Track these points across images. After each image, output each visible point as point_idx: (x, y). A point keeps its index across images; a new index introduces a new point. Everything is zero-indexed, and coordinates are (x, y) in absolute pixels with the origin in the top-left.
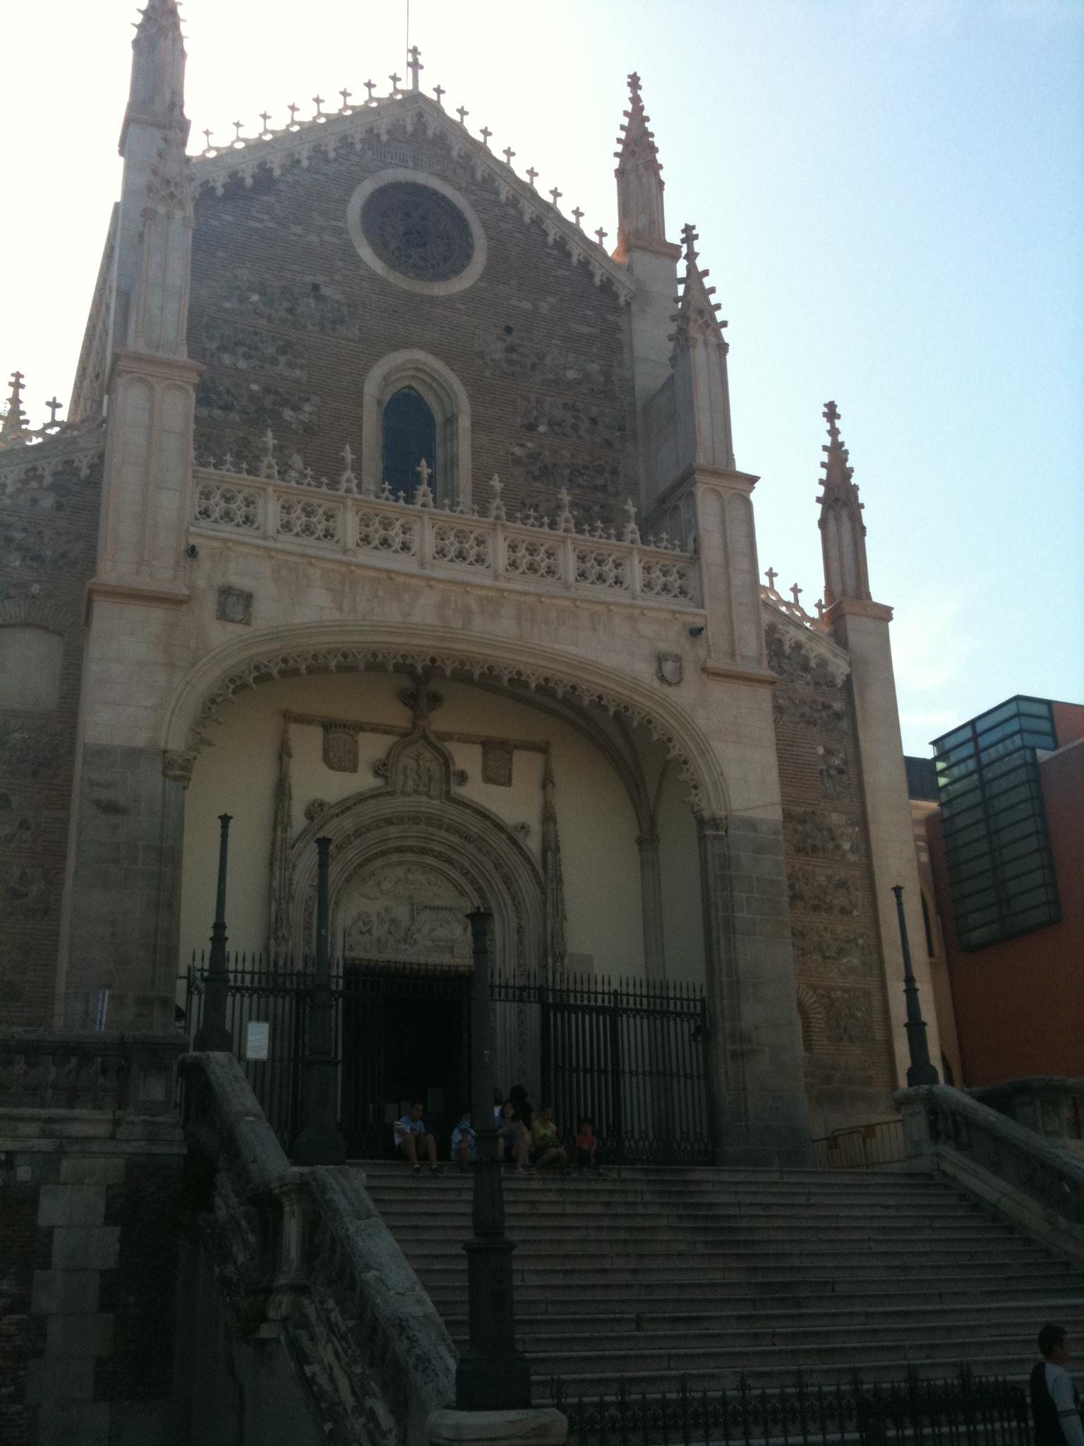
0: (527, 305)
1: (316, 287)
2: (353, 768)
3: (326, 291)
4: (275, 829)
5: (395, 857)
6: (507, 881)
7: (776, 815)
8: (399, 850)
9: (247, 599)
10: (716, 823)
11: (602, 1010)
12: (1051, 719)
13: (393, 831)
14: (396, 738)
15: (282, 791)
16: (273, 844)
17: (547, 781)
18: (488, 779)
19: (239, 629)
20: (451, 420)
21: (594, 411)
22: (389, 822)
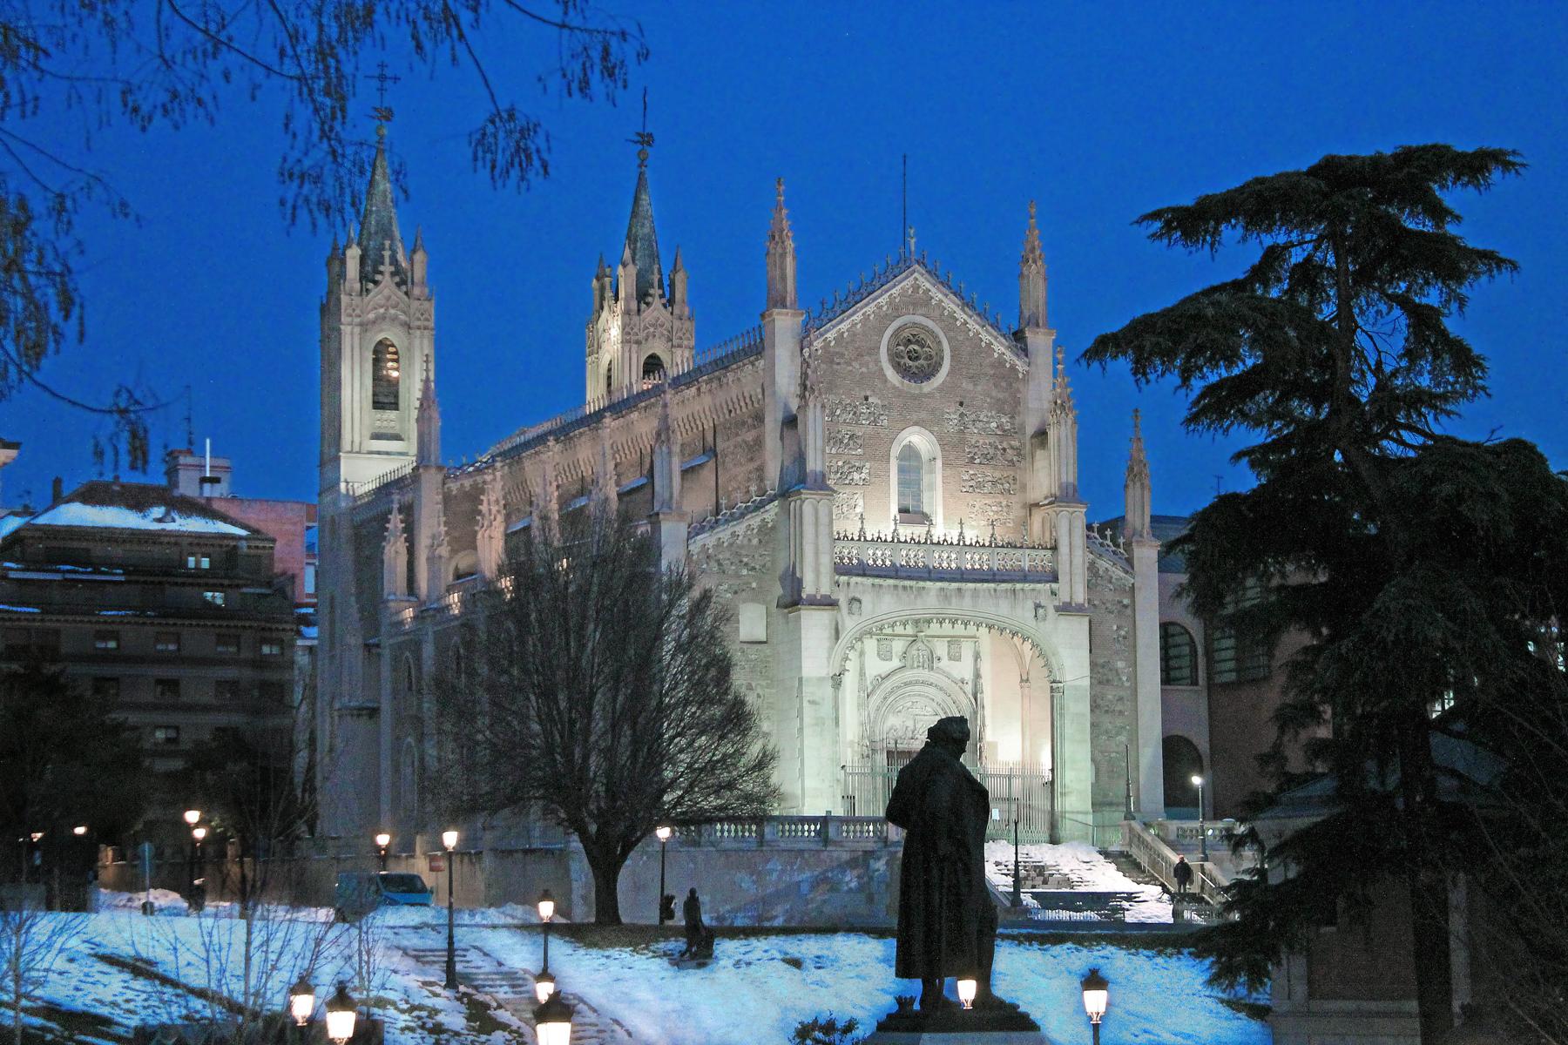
17: (977, 657)
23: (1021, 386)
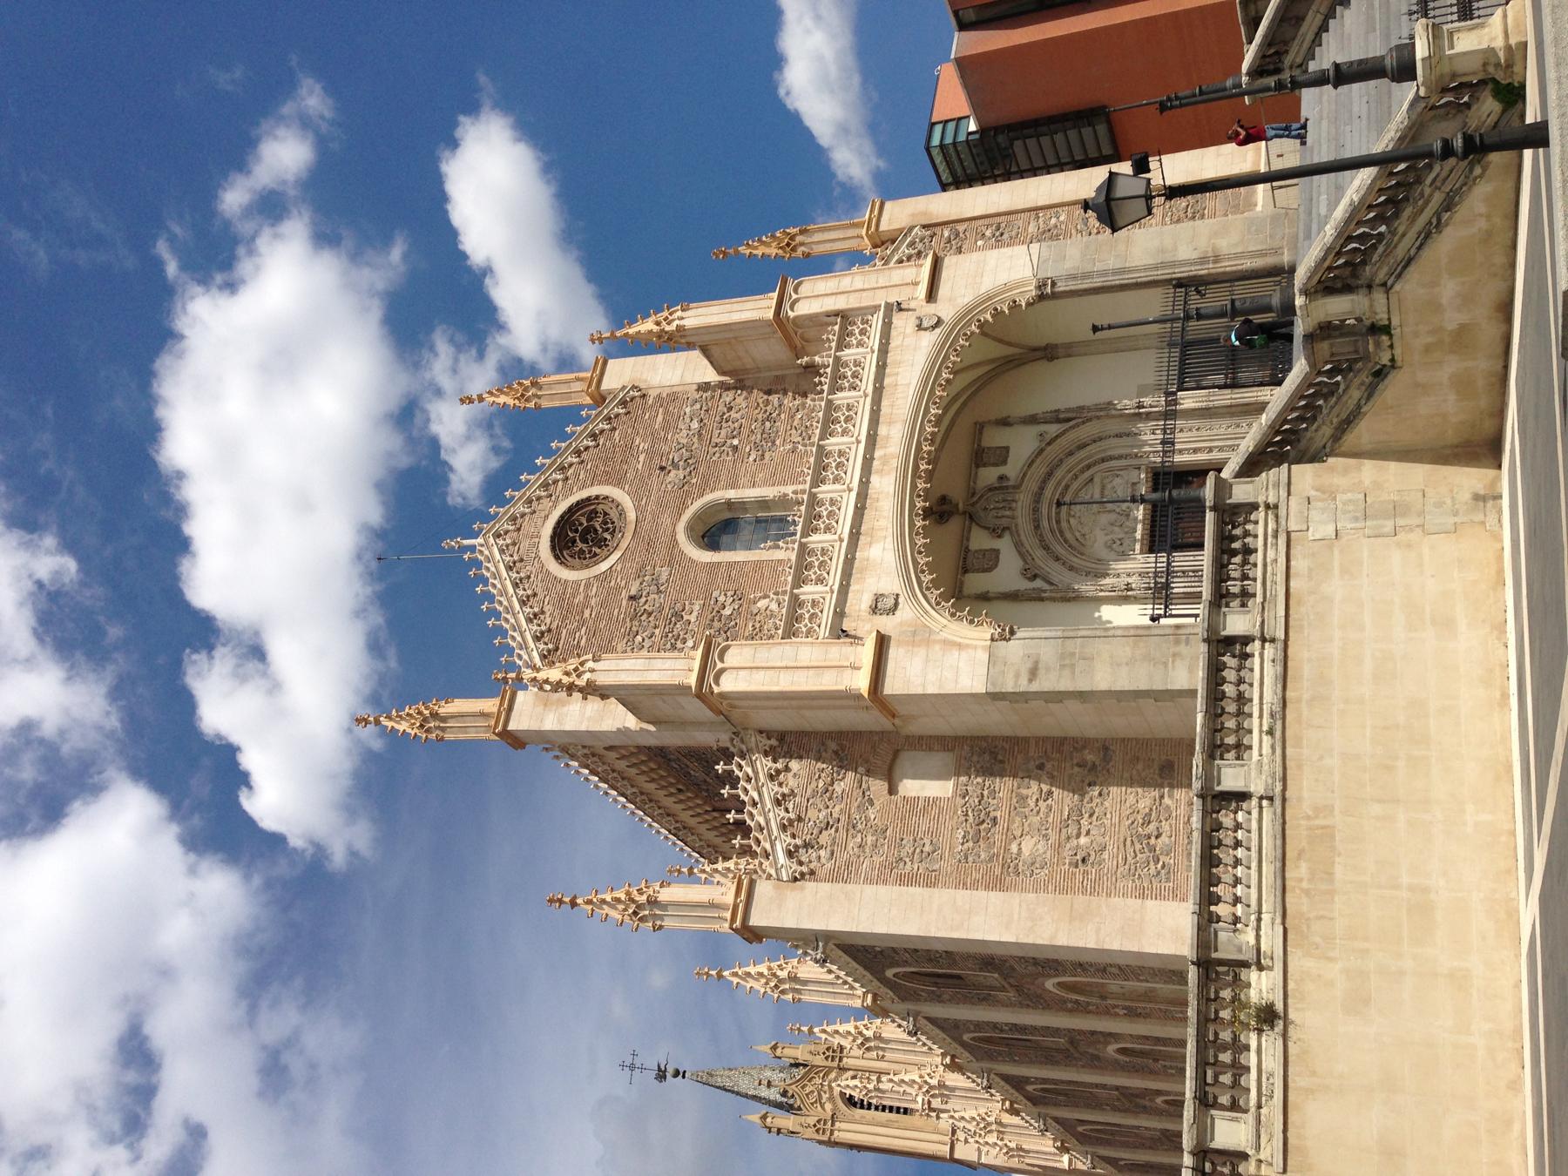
0: (642, 458)
1: (632, 598)
2: (997, 552)
3: (633, 592)
4: (1042, 599)
5: (1064, 524)
6: (1085, 446)
7: (1035, 247)
8: (1058, 522)
9: (878, 598)
10: (1041, 286)
11: (1183, 354)
12: (947, 122)
13: (1045, 523)
14: (975, 529)
15: (1014, 597)
16: (1053, 599)
17: (1005, 422)
18: (1004, 462)
19: (901, 600)
20: (729, 504)
21: (722, 408)
22: (1037, 527)
23: (653, 393)
